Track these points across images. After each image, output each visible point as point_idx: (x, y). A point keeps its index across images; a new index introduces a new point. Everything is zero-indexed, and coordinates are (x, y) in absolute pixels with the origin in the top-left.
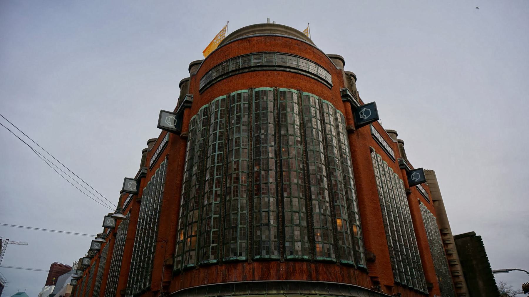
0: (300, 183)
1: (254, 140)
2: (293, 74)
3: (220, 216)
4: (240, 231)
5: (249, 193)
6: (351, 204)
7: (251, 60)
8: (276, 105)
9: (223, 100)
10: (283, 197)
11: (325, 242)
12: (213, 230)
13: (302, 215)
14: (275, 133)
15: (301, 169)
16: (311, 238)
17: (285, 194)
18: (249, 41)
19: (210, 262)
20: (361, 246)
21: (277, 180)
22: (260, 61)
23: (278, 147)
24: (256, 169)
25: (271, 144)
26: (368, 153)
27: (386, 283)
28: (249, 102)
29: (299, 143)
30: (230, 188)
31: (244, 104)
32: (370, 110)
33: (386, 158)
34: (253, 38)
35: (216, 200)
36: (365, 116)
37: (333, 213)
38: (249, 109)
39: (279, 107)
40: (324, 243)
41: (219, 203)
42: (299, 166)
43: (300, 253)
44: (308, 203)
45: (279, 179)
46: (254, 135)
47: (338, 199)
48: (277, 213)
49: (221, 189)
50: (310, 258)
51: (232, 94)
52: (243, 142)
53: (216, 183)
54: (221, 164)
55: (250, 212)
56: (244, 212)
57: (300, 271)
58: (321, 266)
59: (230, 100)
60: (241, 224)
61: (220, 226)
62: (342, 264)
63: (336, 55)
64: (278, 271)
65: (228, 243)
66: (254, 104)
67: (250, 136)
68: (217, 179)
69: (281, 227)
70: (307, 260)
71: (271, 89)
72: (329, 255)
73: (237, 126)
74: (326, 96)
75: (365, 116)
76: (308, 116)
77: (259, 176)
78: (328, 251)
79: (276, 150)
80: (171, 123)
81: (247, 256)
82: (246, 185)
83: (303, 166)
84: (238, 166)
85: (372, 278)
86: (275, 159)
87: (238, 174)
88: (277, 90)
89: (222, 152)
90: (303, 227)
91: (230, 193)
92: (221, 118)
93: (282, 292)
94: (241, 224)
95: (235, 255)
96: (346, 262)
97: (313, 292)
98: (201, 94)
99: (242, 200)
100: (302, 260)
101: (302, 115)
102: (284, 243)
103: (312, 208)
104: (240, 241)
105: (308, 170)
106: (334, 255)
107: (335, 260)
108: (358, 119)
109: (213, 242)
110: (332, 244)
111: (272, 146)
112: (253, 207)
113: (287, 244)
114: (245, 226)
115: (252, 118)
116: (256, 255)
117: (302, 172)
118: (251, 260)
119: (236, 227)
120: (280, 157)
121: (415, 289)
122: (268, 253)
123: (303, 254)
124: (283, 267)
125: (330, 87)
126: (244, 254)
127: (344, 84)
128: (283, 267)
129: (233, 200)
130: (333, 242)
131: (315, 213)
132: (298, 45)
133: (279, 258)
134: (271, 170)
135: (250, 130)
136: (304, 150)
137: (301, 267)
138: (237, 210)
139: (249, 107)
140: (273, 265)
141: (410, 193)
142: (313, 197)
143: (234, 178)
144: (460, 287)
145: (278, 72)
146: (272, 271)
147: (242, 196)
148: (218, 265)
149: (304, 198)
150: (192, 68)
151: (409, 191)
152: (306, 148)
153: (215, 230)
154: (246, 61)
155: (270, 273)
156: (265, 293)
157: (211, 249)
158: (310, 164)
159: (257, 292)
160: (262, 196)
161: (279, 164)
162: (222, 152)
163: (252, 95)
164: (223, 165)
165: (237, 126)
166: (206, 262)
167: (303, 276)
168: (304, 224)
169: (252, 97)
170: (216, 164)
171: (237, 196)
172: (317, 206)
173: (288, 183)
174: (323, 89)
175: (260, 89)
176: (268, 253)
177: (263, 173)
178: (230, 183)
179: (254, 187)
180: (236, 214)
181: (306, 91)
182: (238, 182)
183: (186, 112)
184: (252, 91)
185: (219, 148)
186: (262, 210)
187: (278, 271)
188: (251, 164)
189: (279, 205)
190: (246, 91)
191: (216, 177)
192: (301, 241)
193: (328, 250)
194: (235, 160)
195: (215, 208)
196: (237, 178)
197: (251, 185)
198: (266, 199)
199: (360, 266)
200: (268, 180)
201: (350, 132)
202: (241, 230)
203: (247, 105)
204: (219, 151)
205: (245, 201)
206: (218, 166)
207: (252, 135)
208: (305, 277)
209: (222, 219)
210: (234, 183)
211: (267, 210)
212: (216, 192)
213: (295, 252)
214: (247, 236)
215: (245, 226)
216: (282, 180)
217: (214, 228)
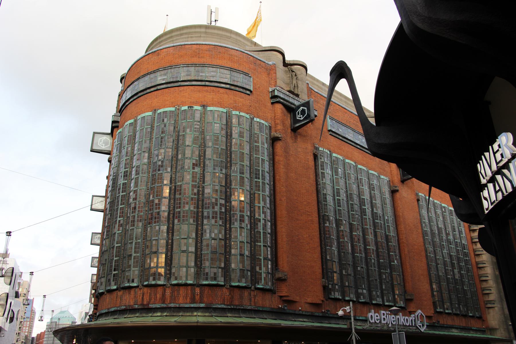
0: (192, 209)
1: (152, 166)
2: (199, 87)
3: (121, 245)
4: (134, 259)
6: (257, 224)
8: (176, 126)
9: (131, 124)
11: (212, 266)
12: (115, 259)
13: (190, 241)
14: (172, 158)
15: (195, 194)
16: (198, 263)
17: (176, 221)
19: (112, 288)
20: (264, 266)
21: (169, 207)
22: (165, 77)
23: (174, 173)
24: (151, 198)
25: (166, 169)
26: (309, 157)
27: (309, 300)
28: (151, 125)
29: (197, 165)
30: (129, 217)
32: (306, 108)
33: (356, 154)
34: (162, 51)
35: (119, 230)
36: (302, 116)
37: (228, 236)
38: (151, 133)
39: (179, 128)
40: (211, 268)
41: (122, 232)
43: (184, 279)
44: (199, 228)
45: (172, 206)
46: (152, 161)
47: (236, 220)
48: (166, 241)
49: (124, 218)
50: (195, 283)
52: (142, 170)
53: (120, 212)
54: (125, 193)
55: (144, 241)
56: (138, 241)
57: (184, 294)
58: (207, 289)
59: (134, 125)
60: (135, 252)
61: (120, 254)
62: (231, 286)
63: (271, 47)
64: (164, 295)
65: (124, 271)
66: (155, 128)
67: (149, 163)
69: (169, 254)
70: (190, 285)
71: (173, 109)
74: (239, 105)
75: (302, 116)
76: (210, 134)
77: (153, 205)
78: (214, 275)
79: (171, 176)
80: (104, 144)
81: (138, 282)
82: (142, 214)
83: (198, 191)
84: (136, 195)
85: (281, 297)
86: (170, 186)
87: (135, 203)
88: (179, 109)
89: (126, 181)
90: (190, 252)
93: (165, 314)
94: (135, 252)
95: (128, 282)
96: (237, 284)
97: (195, 314)
99: (137, 230)
100: (186, 285)
101: (204, 134)
102: (170, 270)
103: (202, 234)
104: (133, 269)
105: (203, 194)
106: (223, 279)
107: (223, 283)
108: (295, 121)
109: (115, 270)
110: (219, 268)
111: (168, 172)
112: (146, 236)
113: (173, 270)
114: (138, 255)
115: (153, 143)
116: (145, 281)
117: (196, 197)
118: (142, 286)
119: (131, 255)
120: (176, 183)
121: (374, 302)
122: (154, 279)
123: (187, 279)
124: (168, 292)
125: (248, 92)
126: (136, 280)
127: (276, 82)
128: (168, 292)
129: (131, 229)
130: (223, 265)
131: (205, 238)
132: (209, 51)
133: (165, 283)
134: (165, 198)
135: (149, 157)
136: (201, 172)
137: (186, 291)
138: (133, 239)
139: (151, 131)
140: (160, 290)
141: (397, 191)
142: (205, 222)
143: (133, 208)
144: (488, 294)
145: (182, 88)
146: (158, 296)
147: (138, 225)
148: (118, 291)
149: (195, 223)
150: (123, 81)
151: (395, 189)
152: (204, 170)
153: (117, 258)
155: (157, 297)
156: (150, 315)
157: (112, 277)
158: (205, 187)
159: (144, 315)
160: (154, 225)
161: (173, 191)
162: (126, 181)
163: (154, 118)
164: (126, 195)
166: (109, 288)
167: (187, 299)
168: (192, 249)
169: (155, 119)
170: (121, 194)
171: (134, 225)
172: (208, 231)
173: (179, 210)
174: (237, 98)
176: (154, 279)
177: (156, 201)
178: (130, 214)
179: (148, 216)
180: (132, 243)
181: (213, 105)
182: (135, 212)
184: (155, 113)
186: (153, 238)
187: (164, 295)
188: (148, 192)
189: (170, 232)
190: (150, 113)
191: (120, 206)
192: (186, 267)
195: (118, 238)
196: (135, 208)
197: (146, 214)
198: (157, 228)
199: (258, 286)
201: (274, 140)
202: (134, 258)
203: (149, 130)
204: (124, 180)
205: (140, 230)
206: (122, 195)
207: (151, 161)
209: (123, 248)
210: (132, 213)
211: (157, 238)
213: (178, 278)
214: (140, 263)
215: (138, 255)
216: (174, 207)
217: (116, 257)
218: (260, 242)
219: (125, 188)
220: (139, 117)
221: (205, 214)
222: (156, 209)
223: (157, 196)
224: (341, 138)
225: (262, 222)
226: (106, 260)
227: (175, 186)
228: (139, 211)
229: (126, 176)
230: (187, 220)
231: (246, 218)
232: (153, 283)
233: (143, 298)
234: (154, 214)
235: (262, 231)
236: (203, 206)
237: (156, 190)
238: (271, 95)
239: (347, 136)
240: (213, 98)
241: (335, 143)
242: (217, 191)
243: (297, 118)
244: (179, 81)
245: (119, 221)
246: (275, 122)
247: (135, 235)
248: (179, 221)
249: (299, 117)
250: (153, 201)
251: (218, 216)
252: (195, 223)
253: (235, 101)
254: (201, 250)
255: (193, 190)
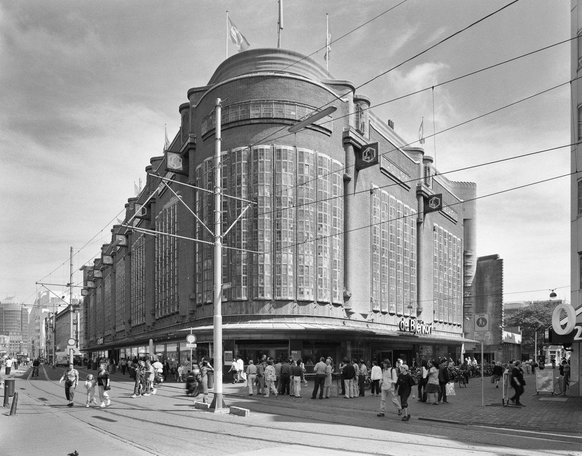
15: (292, 228)
42: (290, 225)
51: (234, 150)
66: (252, 164)
73: (238, 186)
98: (204, 141)
117: (292, 231)
149: (292, 253)
165: (238, 186)
175: (260, 147)
183: (191, 154)
218: (336, 268)
220: (234, 150)
224: (388, 175)
225: (338, 252)
231: (328, 250)
235: (337, 260)
239: (393, 173)
241: (384, 180)
242: (308, 227)
243: (363, 160)
246: (346, 162)
249: (365, 158)
251: (310, 248)
252: (292, 253)
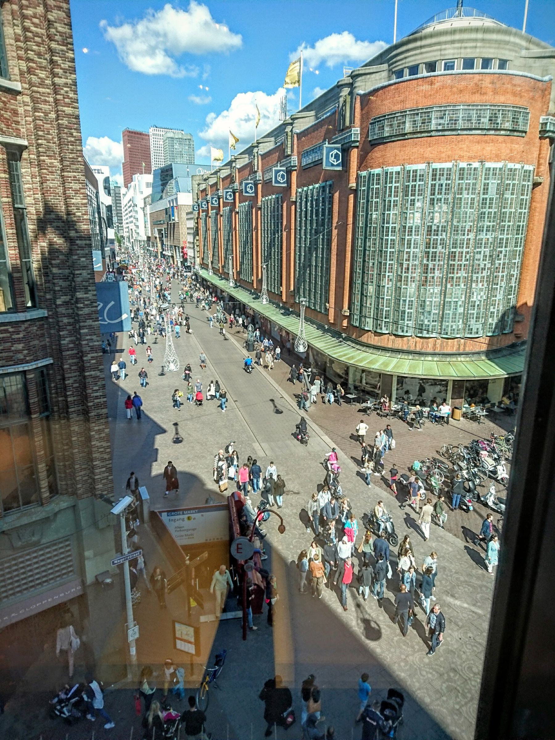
1: (426, 229)
5: (417, 283)
7: (431, 119)
10: (446, 287)
17: (449, 286)
18: (432, 83)
22: (442, 121)
31: (419, 185)
34: (436, 78)
35: (388, 284)
42: (466, 257)
54: (393, 250)
60: (409, 309)
68: (389, 264)
72: (477, 333)
77: (427, 269)
82: (415, 275)
84: (409, 257)
87: (408, 265)
89: (394, 238)
91: (401, 281)
92: (394, 197)
109: (386, 318)
125: (524, 134)
142: (474, 285)
154: (425, 120)
170: (389, 250)
171: (407, 285)
178: (402, 272)
182: (408, 273)
185: (392, 232)
187: (435, 345)
193: (478, 329)
194: (406, 250)
195: (388, 292)
196: (408, 269)
200: (434, 273)
208: (455, 349)
210: (405, 272)
212: (389, 276)
219: (394, 244)
221: (474, 278)
222: (431, 273)
223: (432, 261)
226: (371, 304)
227: (449, 252)
228: (412, 273)
229: (395, 232)
230: (459, 285)
232: (427, 336)
233: (416, 346)
234: (429, 278)
236: (472, 271)
237: (430, 255)
238: (542, 128)
240: (491, 150)
244: (458, 130)
245: (389, 276)
246: (539, 161)
247: (408, 294)
248: (452, 285)
250: (428, 265)
253: (511, 150)
254: (468, 310)
255: (466, 257)
